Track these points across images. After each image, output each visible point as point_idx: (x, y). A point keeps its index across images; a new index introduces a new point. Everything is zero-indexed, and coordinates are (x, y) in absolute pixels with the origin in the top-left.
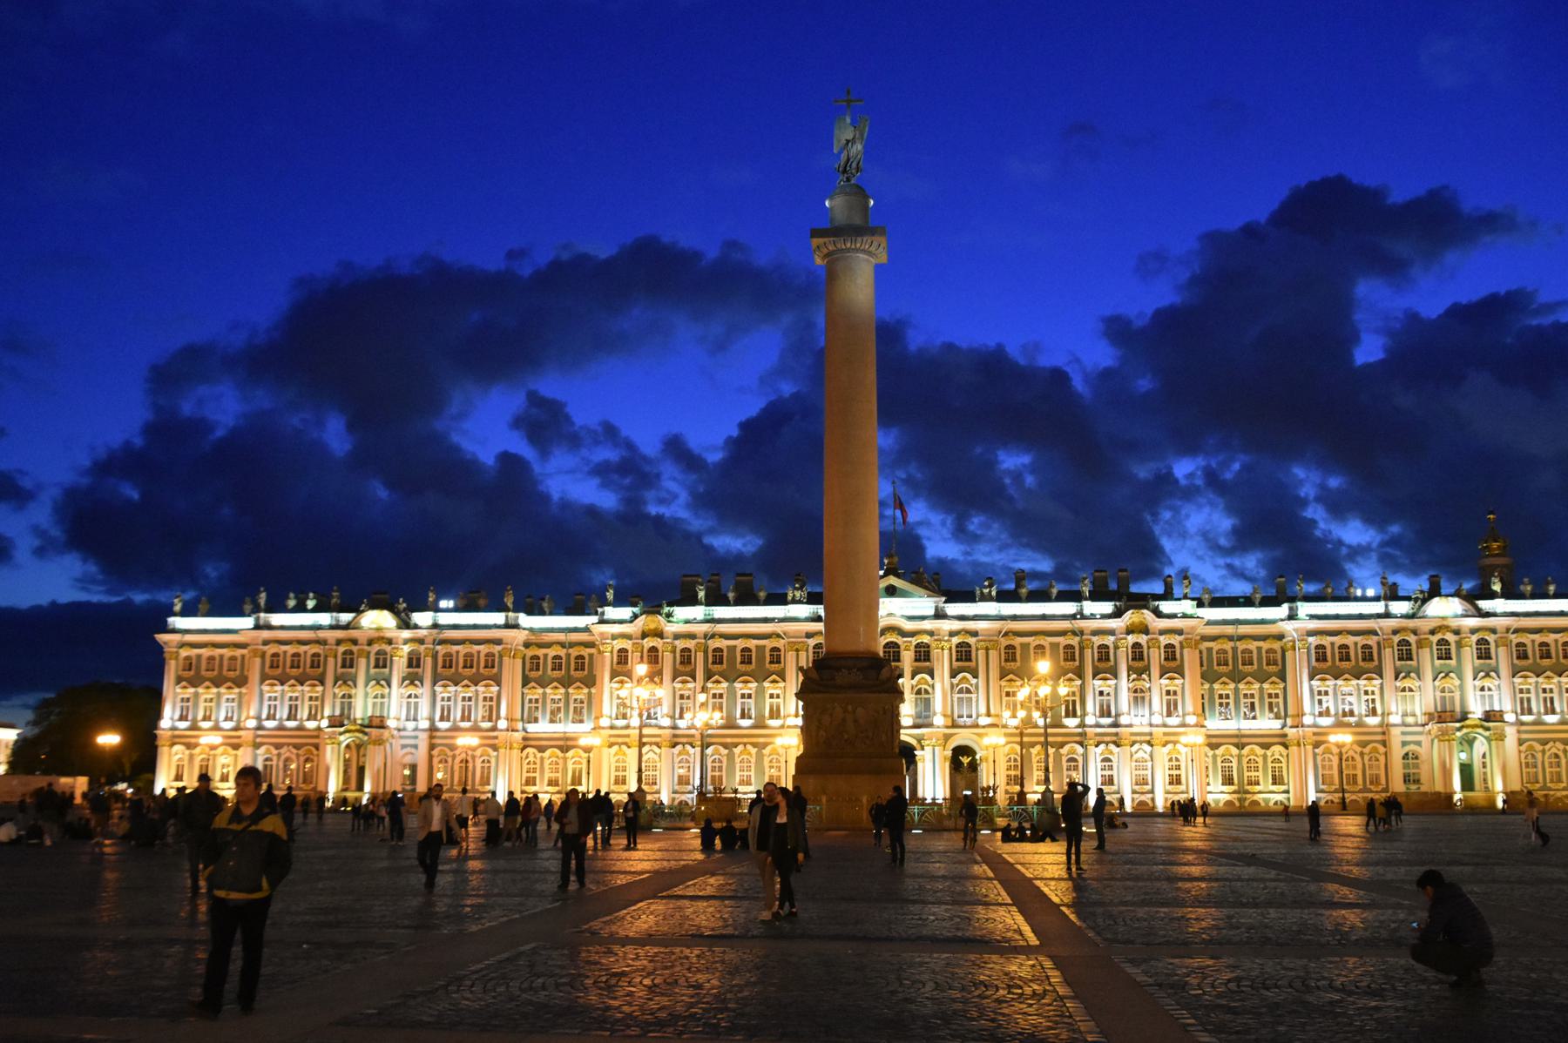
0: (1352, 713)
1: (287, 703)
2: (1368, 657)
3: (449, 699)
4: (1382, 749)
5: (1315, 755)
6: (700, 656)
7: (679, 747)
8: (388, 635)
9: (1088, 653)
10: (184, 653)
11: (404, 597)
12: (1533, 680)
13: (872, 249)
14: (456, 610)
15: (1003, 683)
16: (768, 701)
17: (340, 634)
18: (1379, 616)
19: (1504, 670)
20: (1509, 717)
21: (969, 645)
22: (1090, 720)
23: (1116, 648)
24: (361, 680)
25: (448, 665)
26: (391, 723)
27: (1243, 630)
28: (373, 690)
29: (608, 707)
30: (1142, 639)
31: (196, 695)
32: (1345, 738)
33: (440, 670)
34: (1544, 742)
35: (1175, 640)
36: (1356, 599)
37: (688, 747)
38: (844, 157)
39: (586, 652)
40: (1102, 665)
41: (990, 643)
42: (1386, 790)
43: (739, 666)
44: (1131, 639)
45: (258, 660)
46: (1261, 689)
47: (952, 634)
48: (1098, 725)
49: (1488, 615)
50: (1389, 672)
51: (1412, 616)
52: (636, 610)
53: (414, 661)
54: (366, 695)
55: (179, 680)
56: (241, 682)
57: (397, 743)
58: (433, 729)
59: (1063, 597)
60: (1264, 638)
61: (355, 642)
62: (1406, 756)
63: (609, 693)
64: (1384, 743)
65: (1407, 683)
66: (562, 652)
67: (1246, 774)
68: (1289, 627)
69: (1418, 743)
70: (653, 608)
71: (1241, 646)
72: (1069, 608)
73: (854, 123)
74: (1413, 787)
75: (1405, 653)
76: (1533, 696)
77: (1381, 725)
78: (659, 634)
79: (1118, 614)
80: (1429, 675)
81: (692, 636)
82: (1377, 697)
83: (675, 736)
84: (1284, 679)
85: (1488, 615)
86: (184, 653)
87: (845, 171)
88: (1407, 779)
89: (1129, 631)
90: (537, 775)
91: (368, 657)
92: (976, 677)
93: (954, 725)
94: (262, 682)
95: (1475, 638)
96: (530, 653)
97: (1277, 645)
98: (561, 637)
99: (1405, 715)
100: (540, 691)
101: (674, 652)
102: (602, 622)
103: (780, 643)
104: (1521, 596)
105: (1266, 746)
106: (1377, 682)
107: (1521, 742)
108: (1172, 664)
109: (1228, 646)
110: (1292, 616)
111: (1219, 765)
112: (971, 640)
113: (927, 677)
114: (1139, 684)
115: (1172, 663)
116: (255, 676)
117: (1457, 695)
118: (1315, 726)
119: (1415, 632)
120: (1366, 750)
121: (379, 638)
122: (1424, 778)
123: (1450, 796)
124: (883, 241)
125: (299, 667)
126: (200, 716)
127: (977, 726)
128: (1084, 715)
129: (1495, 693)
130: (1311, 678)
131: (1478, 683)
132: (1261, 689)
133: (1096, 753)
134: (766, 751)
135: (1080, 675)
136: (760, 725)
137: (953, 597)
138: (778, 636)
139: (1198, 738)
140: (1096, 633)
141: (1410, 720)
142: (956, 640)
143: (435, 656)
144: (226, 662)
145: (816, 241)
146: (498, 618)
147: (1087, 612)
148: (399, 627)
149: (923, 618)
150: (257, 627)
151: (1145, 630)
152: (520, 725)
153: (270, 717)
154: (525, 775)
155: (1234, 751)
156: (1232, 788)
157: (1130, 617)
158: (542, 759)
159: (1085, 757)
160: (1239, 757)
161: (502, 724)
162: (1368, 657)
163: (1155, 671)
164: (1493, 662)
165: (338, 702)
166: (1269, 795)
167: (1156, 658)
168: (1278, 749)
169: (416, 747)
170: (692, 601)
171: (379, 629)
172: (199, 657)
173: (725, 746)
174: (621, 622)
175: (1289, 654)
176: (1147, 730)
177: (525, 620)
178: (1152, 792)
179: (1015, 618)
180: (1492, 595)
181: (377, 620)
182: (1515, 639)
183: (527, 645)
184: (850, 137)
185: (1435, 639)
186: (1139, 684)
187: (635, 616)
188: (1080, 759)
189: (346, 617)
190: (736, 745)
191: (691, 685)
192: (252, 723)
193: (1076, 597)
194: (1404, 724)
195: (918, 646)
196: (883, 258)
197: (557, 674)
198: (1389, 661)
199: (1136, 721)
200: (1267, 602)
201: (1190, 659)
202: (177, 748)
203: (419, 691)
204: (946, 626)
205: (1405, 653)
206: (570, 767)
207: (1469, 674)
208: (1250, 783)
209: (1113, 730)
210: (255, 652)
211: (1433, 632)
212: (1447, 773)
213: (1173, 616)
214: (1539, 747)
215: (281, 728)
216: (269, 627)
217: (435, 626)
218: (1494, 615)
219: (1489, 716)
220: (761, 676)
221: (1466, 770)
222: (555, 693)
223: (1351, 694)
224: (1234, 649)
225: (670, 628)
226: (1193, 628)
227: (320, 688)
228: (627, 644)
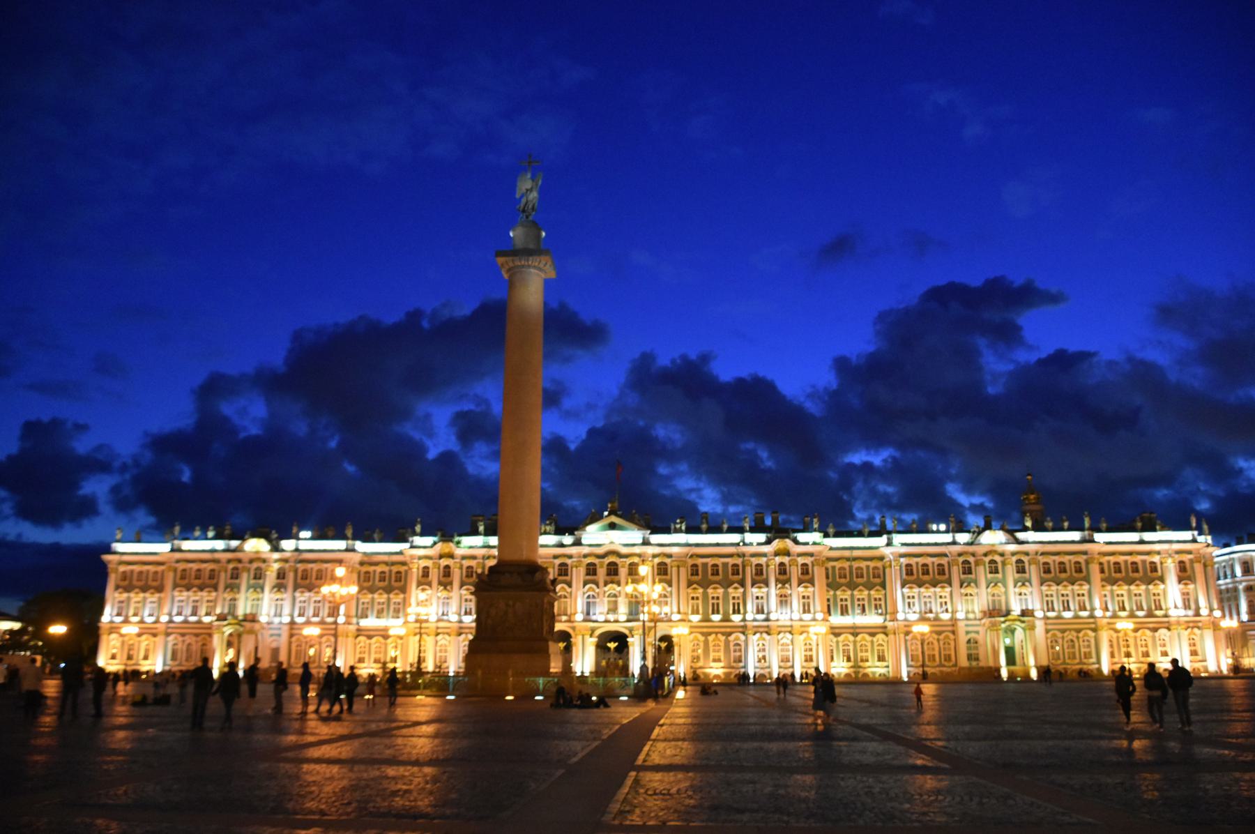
0: (931, 612)
1: (191, 605)
2: (942, 572)
4: (952, 636)
5: (906, 641)
8: (264, 556)
9: (748, 569)
10: (122, 568)
11: (276, 530)
12: (1054, 588)
13: (541, 265)
14: (313, 538)
15: (690, 590)
17: (229, 555)
18: (948, 544)
19: (1035, 580)
20: (1039, 614)
21: (665, 564)
22: (749, 616)
23: (768, 566)
24: (243, 587)
25: (304, 577)
26: (263, 619)
28: (252, 595)
29: (413, 610)
30: (786, 560)
31: (129, 599)
32: (924, 628)
33: (299, 580)
34: (1063, 631)
35: (808, 560)
36: (933, 532)
38: (524, 200)
39: (403, 569)
40: (757, 578)
41: (680, 561)
42: (955, 665)
44: (778, 559)
45: (171, 575)
46: (869, 595)
47: (654, 556)
48: (755, 620)
49: (1022, 543)
50: (956, 582)
51: (971, 544)
52: (435, 539)
53: (281, 575)
54: (247, 598)
55: (117, 587)
56: (160, 589)
57: (267, 633)
58: (292, 623)
59: (732, 530)
60: (871, 559)
61: (240, 561)
62: (969, 641)
63: (417, 594)
64: (953, 632)
65: (969, 591)
67: (860, 654)
68: (887, 551)
69: (977, 632)
70: (447, 537)
71: (855, 564)
72: (735, 538)
73: (533, 178)
74: (974, 663)
75: (967, 571)
76: (1055, 599)
77: (951, 619)
78: (451, 556)
79: (769, 542)
80: (983, 585)
81: (474, 557)
82: (948, 600)
84: (884, 588)
85: (1022, 543)
86: (122, 568)
87: (524, 211)
88: (970, 657)
89: (777, 554)
90: (366, 656)
91: (249, 570)
92: (670, 585)
95: (1014, 559)
96: (365, 569)
97: (879, 564)
98: (386, 558)
99: (967, 612)
101: (461, 568)
102: (412, 547)
104: (1044, 529)
105: (873, 635)
106: (948, 589)
107: (1047, 631)
108: (807, 577)
109: (846, 565)
110: (889, 544)
111: (841, 648)
112: (668, 561)
114: (783, 591)
115: (806, 576)
116: (169, 583)
117: (1003, 599)
118: (906, 620)
119: (973, 555)
120: (942, 637)
121: (257, 558)
122: (981, 657)
123: (998, 670)
124: (547, 258)
125: (200, 578)
126: (131, 612)
127: (670, 621)
128: (745, 612)
129: (1029, 597)
130: (903, 586)
131: (1017, 590)
132: (869, 595)
135: (742, 584)
137: (655, 530)
139: (822, 629)
140: (754, 555)
141: (971, 616)
142: (657, 560)
143: (296, 571)
145: (500, 260)
146: (341, 544)
147: (747, 541)
149: (634, 545)
150: (173, 550)
151: (787, 553)
152: (354, 620)
153: (179, 614)
154: (358, 656)
155: (851, 638)
156: (850, 664)
157: (777, 544)
160: (855, 642)
161: (341, 619)
162: (942, 572)
163: (794, 581)
164: (1027, 575)
165: (227, 604)
166: (876, 669)
167: (795, 573)
168: (881, 636)
170: (475, 532)
171: (257, 552)
172: (132, 572)
174: (425, 547)
175: (887, 570)
176: (789, 623)
177: (361, 546)
178: (792, 667)
179: (697, 545)
180: (1025, 529)
181: (256, 545)
182: (1042, 559)
183: (362, 564)
184: (529, 186)
185: (987, 559)
186: (783, 591)
187: (435, 543)
189: (234, 543)
192: (164, 619)
193: (740, 530)
194: (967, 619)
196: (552, 274)
197: (382, 584)
198: (956, 573)
199: (781, 617)
200: (872, 534)
201: (819, 573)
202: (114, 636)
203: (284, 596)
204: (650, 550)
205: (967, 571)
208: (862, 661)
209: (765, 623)
210: (170, 568)
211: (985, 555)
212: (996, 654)
213: (807, 544)
214: (1059, 635)
215: (186, 622)
216: (180, 550)
217: (297, 550)
218: (1027, 543)
219: (1024, 613)
221: (1010, 652)
222: (380, 598)
223: (935, 598)
224: (851, 567)
225: (459, 552)
226: (820, 552)
227: (214, 594)
228: (429, 563)
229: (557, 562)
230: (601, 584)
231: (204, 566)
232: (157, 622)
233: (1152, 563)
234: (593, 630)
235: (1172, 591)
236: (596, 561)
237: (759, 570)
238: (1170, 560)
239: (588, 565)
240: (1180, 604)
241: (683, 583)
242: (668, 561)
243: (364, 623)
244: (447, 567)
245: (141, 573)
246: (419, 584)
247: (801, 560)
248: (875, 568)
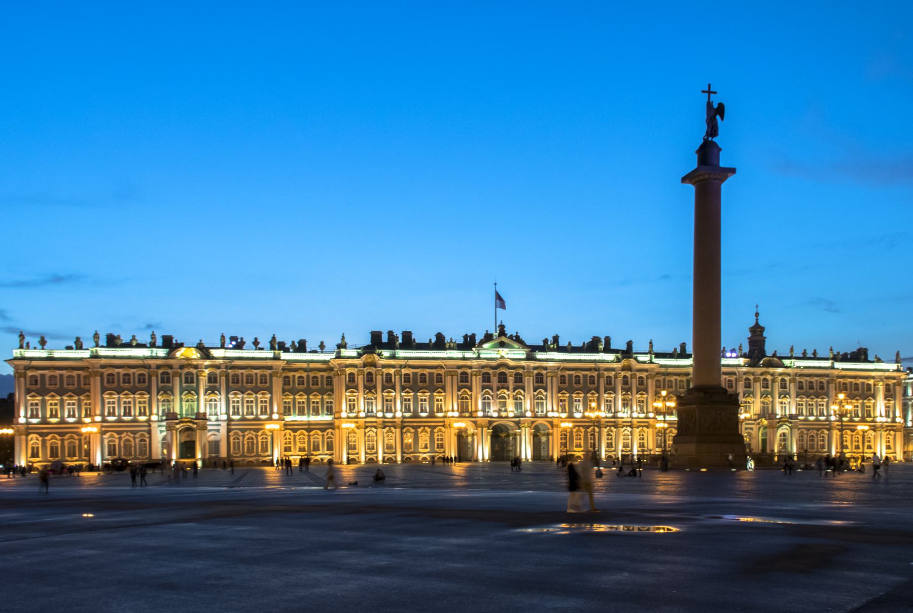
3: (238, 402)
6: (379, 377)
7: (387, 428)
9: (602, 380)
16: (436, 403)
19: (793, 393)
21: (542, 375)
24: (177, 391)
27: (670, 370)
30: (628, 374)
33: (231, 384)
35: (644, 375)
37: (392, 429)
40: (608, 387)
43: (420, 384)
47: (535, 368)
53: (212, 379)
54: (181, 400)
60: (679, 374)
61: (170, 367)
66: (304, 375)
71: (668, 378)
79: (619, 360)
80: (759, 395)
83: (384, 422)
89: (623, 369)
92: (546, 391)
93: (536, 417)
94: (103, 392)
95: (780, 378)
98: (305, 365)
100: (292, 397)
101: (382, 375)
103: (442, 372)
108: (642, 387)
112: (544, 372)
113: (542, 391)
133: (636, 431)
134: (436, 430)
135: (598, 391)
136: (432, 415)
138: (442, 367)
140: (607, 370)
142: (535, 372)
143: (227, 376)
144: (65, 379)
148: (202, 358)
157: (624, 362)
158: (295, 436)
159: (600, 433)
163: (634, 390)
167: (634, 383)
169: (218, 431)
173: (413, 427)
176: (629, 420)
190: (419, 427)
191: (393, 394)
195: (516, 374)
197: (301, 387)
201: (651, 384)
204: (532, 364)
206: (312, 440)
207: (777, 396)
220: (433, 389)
222: (301, 398)
224: (664, 380)
226: (653, 369)
228: (354, 371)
229: (460, 371)
230: (495, 388)
231: (131, 371)
232: (394, 417)
233: (868, 384)
235: (880, 404)
236: (491, 371)
237: (609, 381)
238: (881, 383)
239: (484, 374)
240: (883, 414)
241: (555, 390)
242: (544, 372)
243: (288, 419)
244: (370, 374)
245: (52, 377)
246: (347, 388)
247: (638, 374)
248: (681, 381)
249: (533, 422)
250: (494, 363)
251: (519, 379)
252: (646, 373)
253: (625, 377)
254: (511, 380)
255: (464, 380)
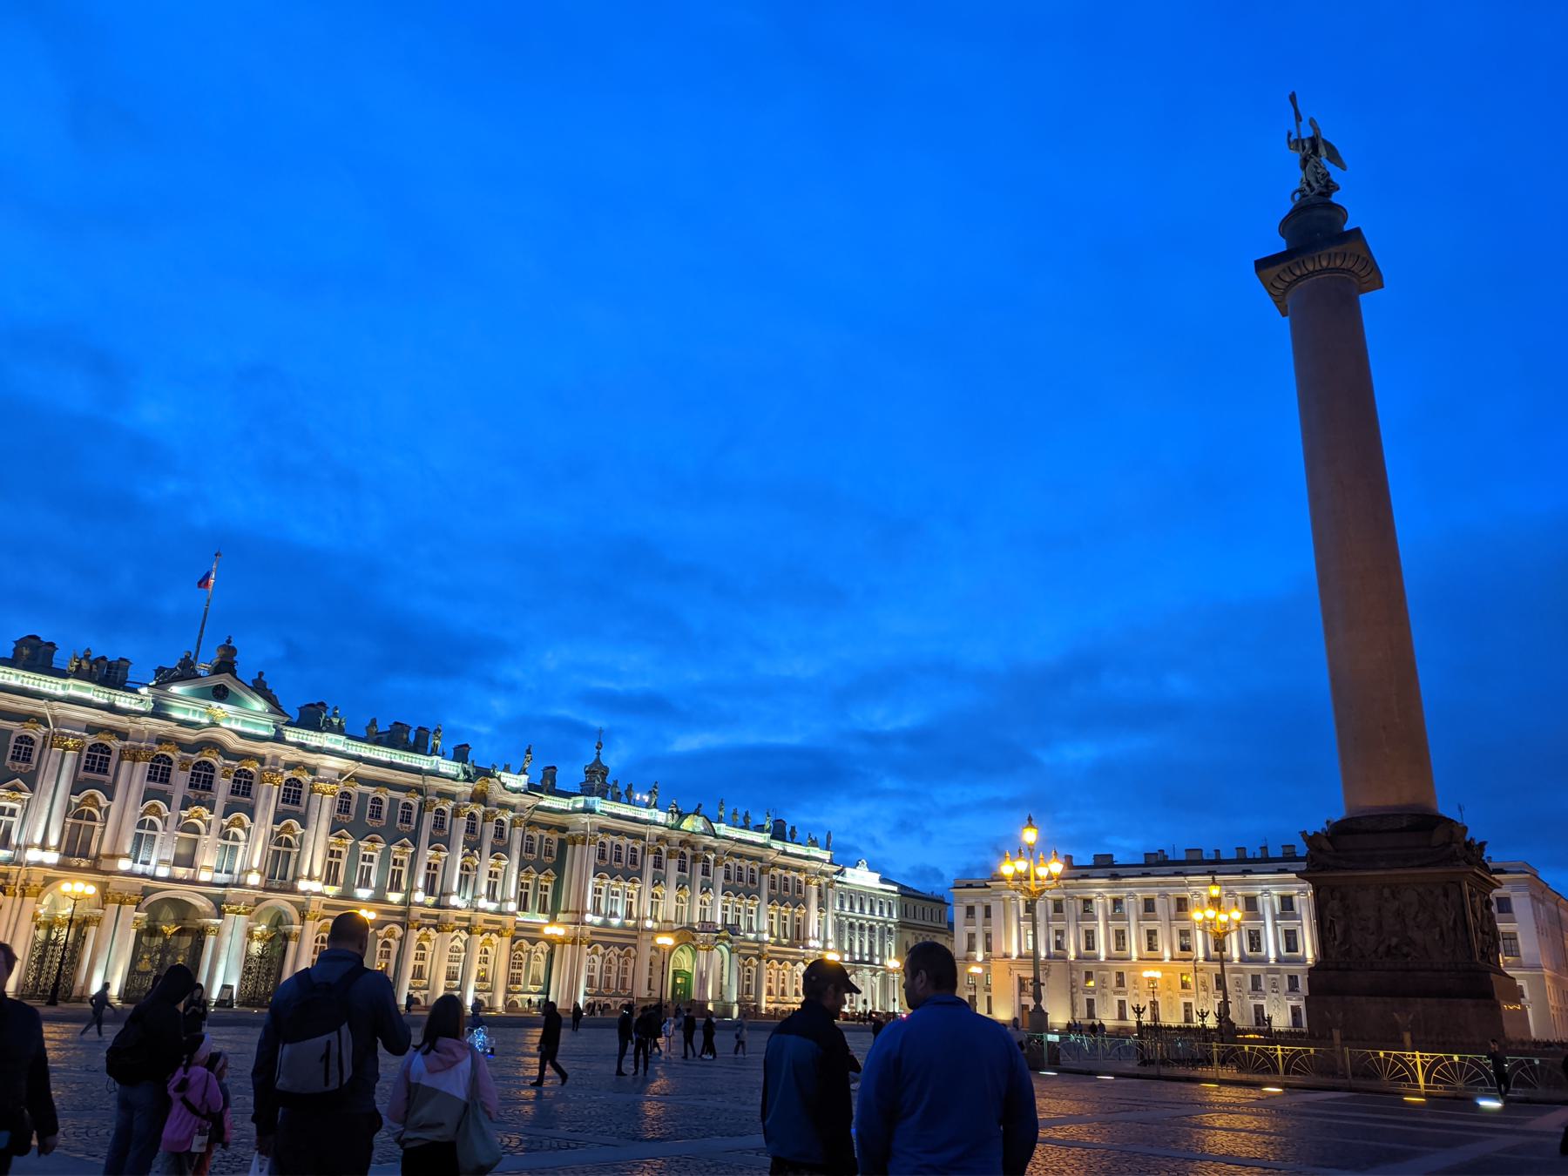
15: (332, 839)
22: (419, 897)
30: (479, 810)
42: (630, 995)
112: (306, 778)
128: (411, 890)
135: (415, 842)
138: (42, 720)
140: (443, 795)
142: (288, 774)
163: (487, 848)
176: (466, 914)
188: (394, 944)
195: (239, 773)
205: (658, 864)
209: (435, 911)
230: (177, 800)
234: (146, 892)
236: (176, 756)
241: (324, 826)
249: (259, 901)
250: (189, 735)
251: (244, 786)
252: (511, 814)
253: (472, 816)
254: (223, 786)
255: (97, 765)
